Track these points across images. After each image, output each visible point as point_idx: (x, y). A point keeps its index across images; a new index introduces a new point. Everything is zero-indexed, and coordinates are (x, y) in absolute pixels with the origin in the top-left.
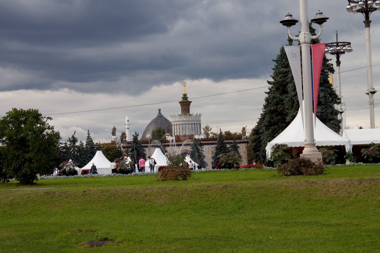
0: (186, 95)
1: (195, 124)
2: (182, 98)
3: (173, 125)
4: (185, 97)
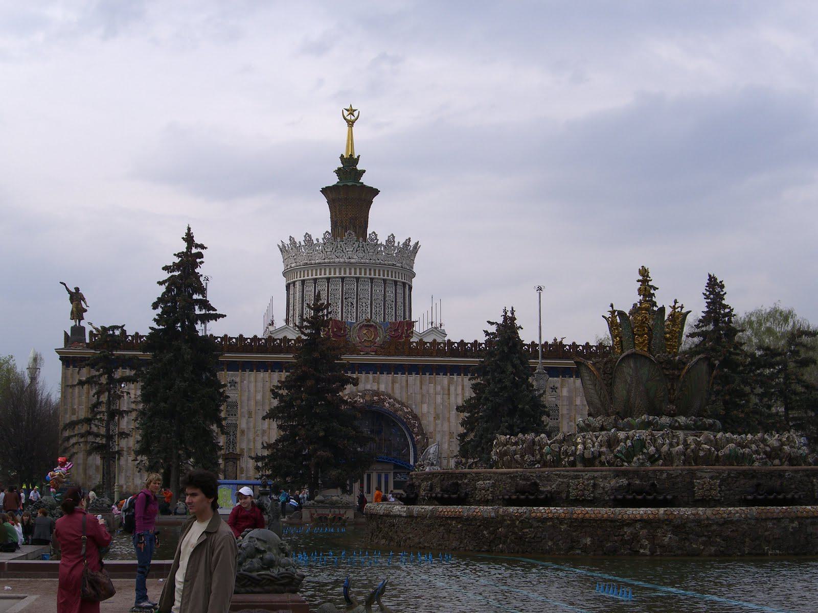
0: (356, 161)
1: (396, 282)
2: (339, 172)
3: (298, 285)
4: (349, 168)
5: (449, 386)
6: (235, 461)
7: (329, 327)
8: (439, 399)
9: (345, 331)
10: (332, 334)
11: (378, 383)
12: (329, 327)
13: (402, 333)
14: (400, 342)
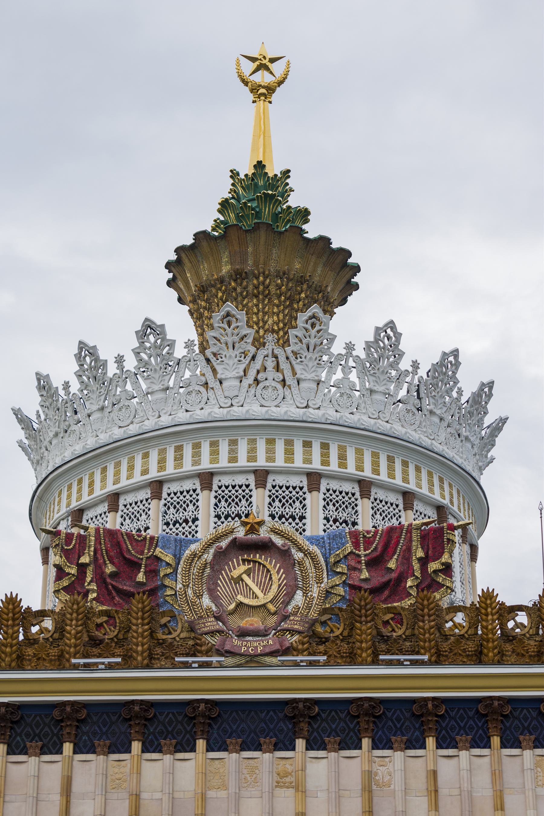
7: (85, 559)
9: (152, 573)
10: (94, 586)
12: (85, 559)
13: (401, 579)
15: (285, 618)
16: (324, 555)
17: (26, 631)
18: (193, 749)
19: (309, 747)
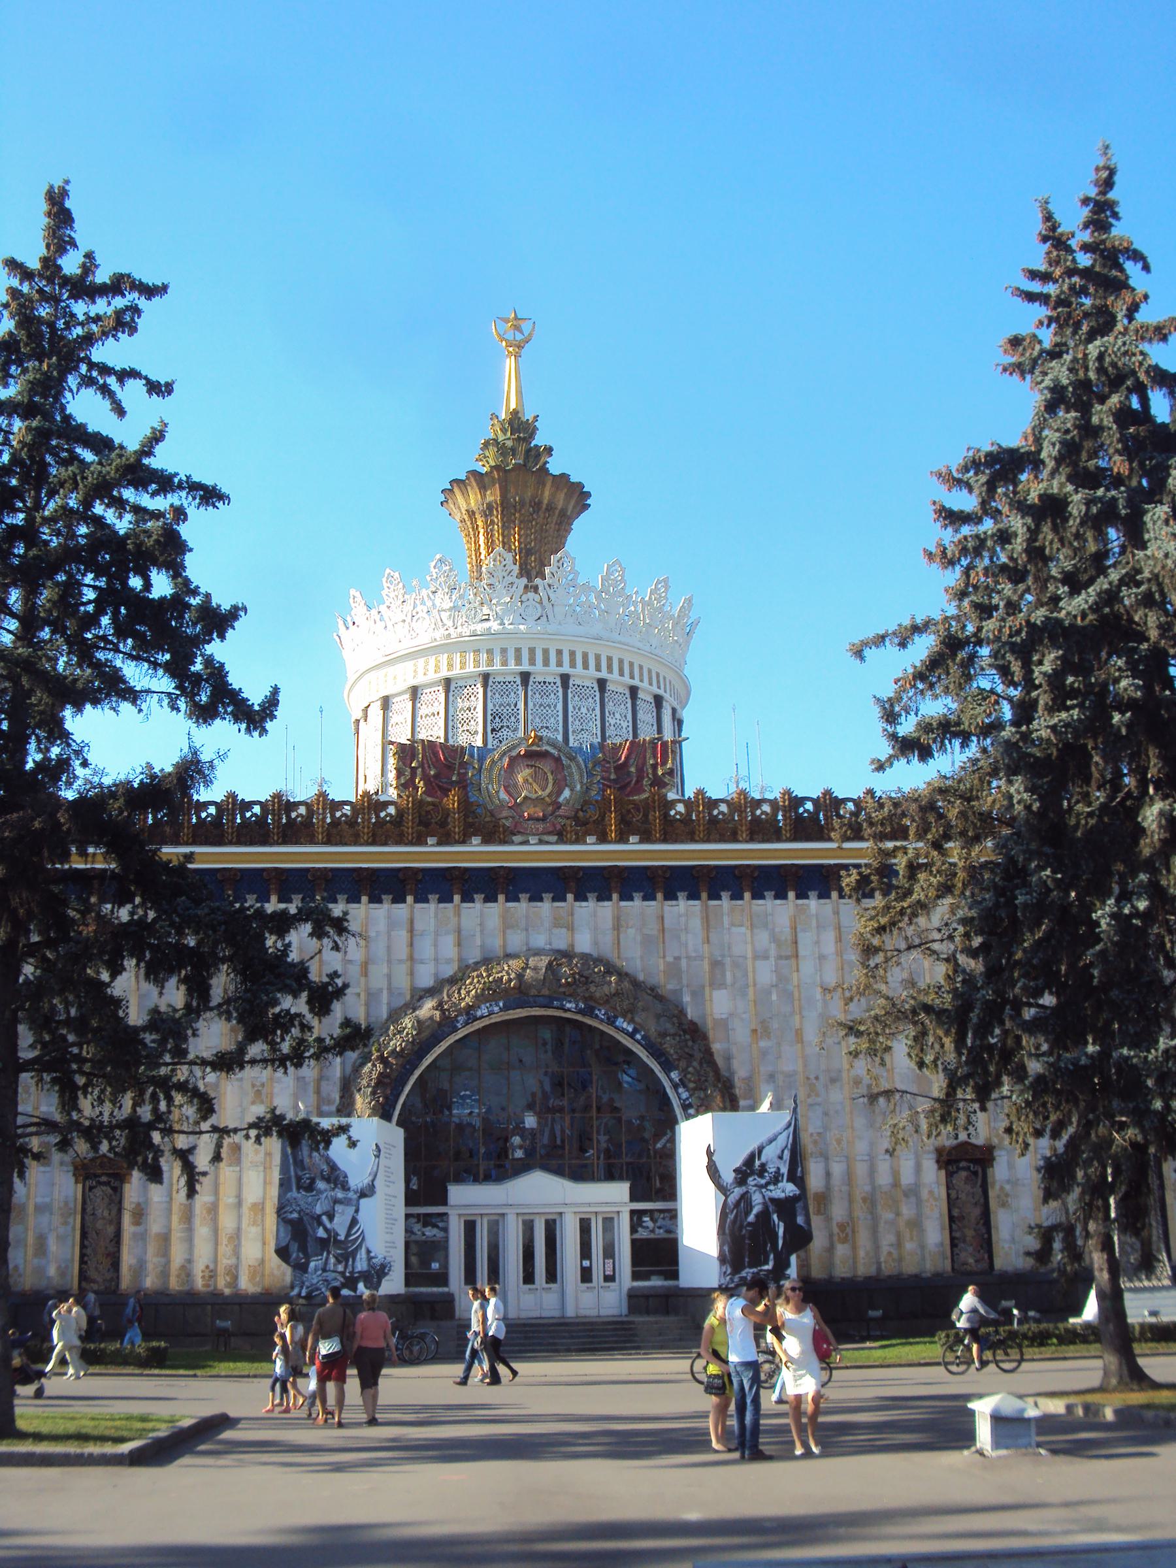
5: (794, 929)
6: (117, 1184)
8: (765, 974)
11: (571, 928)
14: (633, 802)
15: (559, 808)
16: (585, 761)
17: (378, 816)
18: (496, 901)
19: (576, 899)
